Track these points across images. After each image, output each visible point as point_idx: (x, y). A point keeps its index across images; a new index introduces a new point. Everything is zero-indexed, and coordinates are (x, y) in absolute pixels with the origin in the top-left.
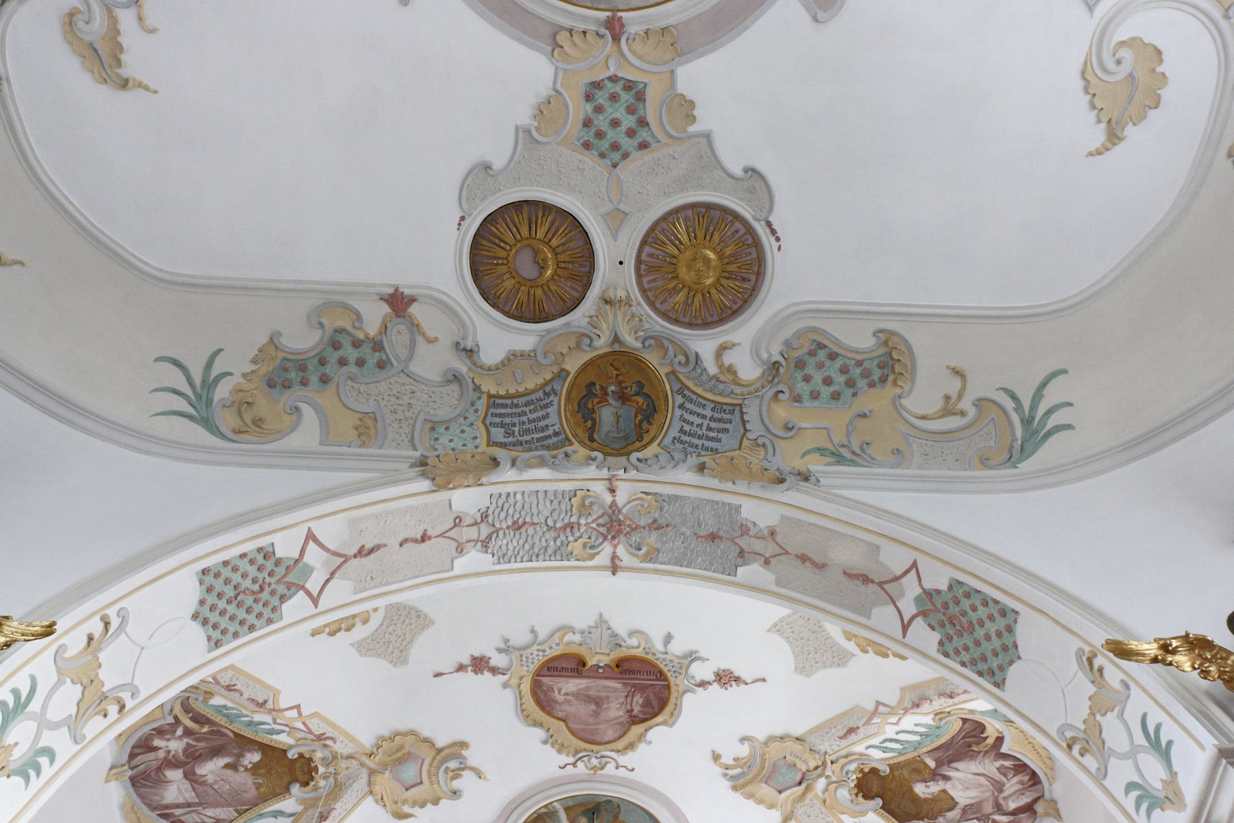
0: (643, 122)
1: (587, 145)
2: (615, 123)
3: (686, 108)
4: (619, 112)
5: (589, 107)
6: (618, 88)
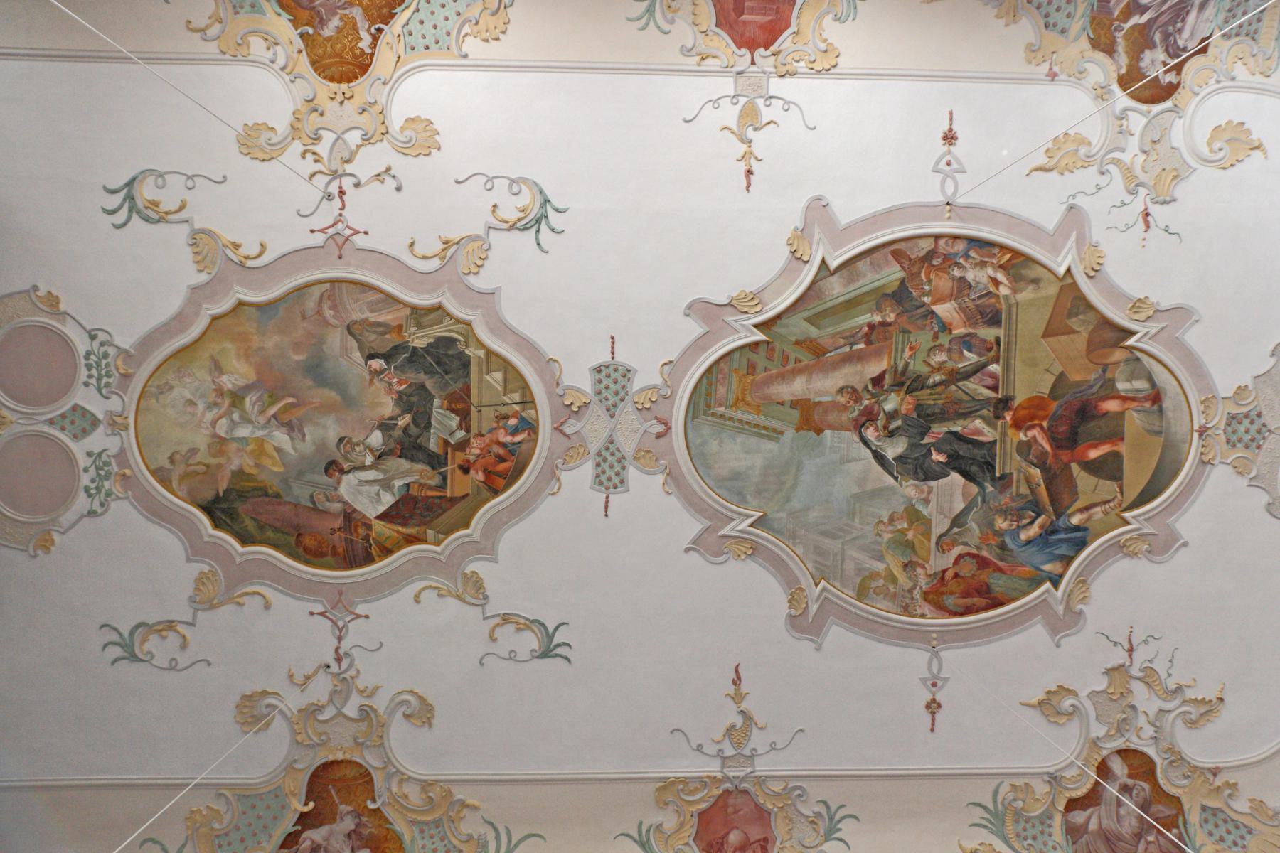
0: (1247, 415)
1: (1259, 447)
2: (1247, 431)
3: (1242, 389)
4: (1242, 429)
5: (1239, 445)
6: (1230, 430)
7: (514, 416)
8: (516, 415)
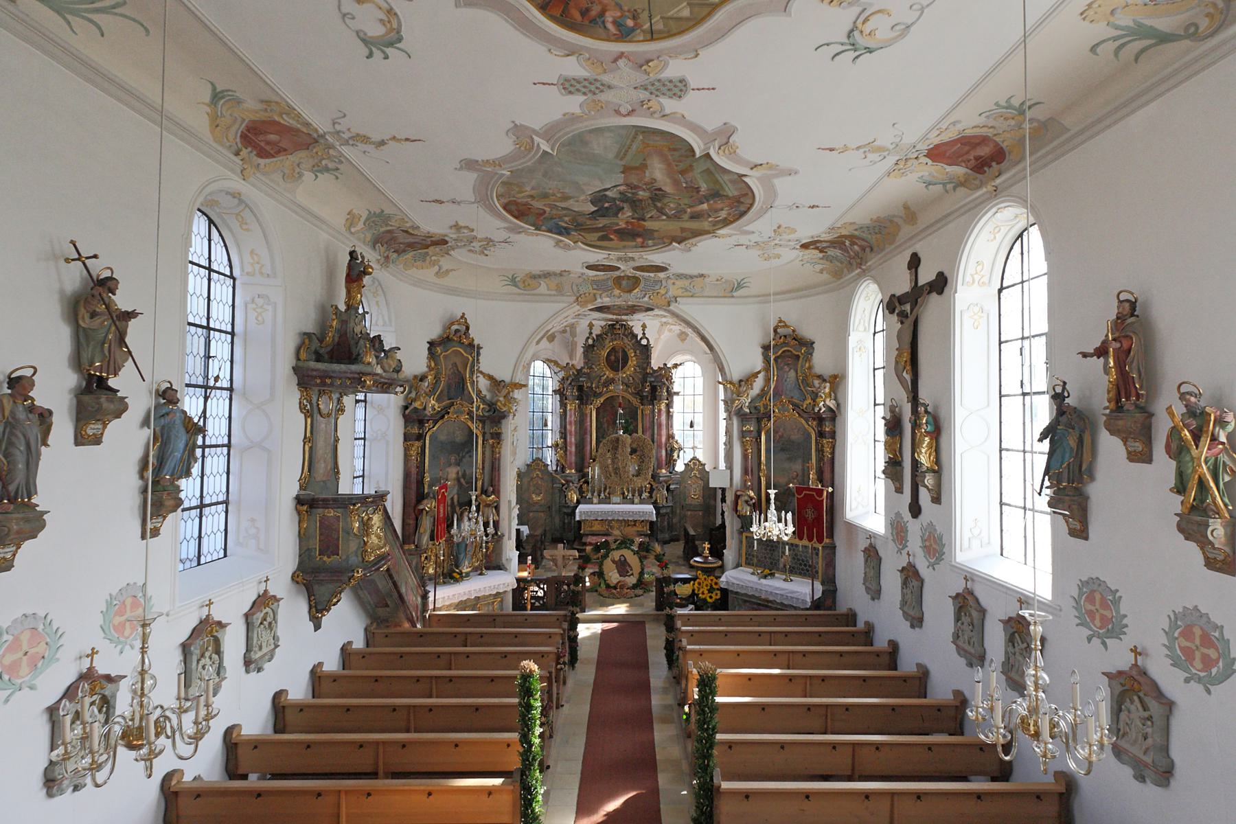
7: (636, 24)
8: (637, 26)
